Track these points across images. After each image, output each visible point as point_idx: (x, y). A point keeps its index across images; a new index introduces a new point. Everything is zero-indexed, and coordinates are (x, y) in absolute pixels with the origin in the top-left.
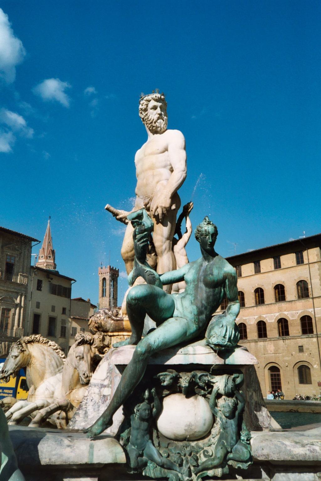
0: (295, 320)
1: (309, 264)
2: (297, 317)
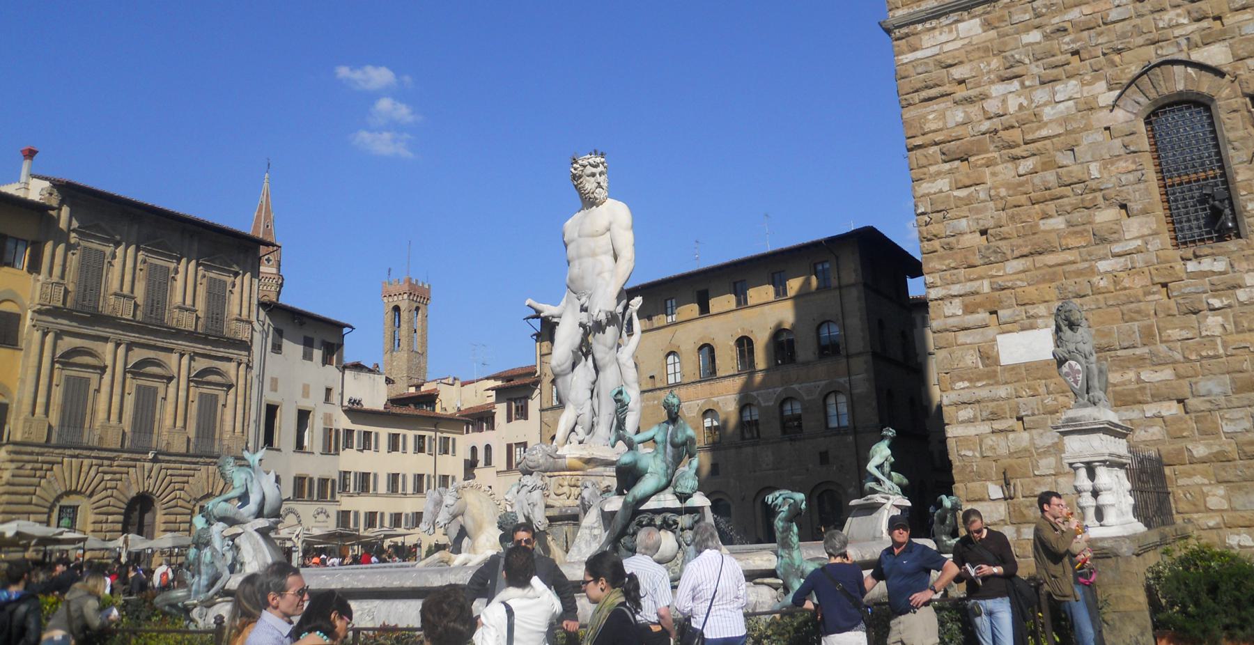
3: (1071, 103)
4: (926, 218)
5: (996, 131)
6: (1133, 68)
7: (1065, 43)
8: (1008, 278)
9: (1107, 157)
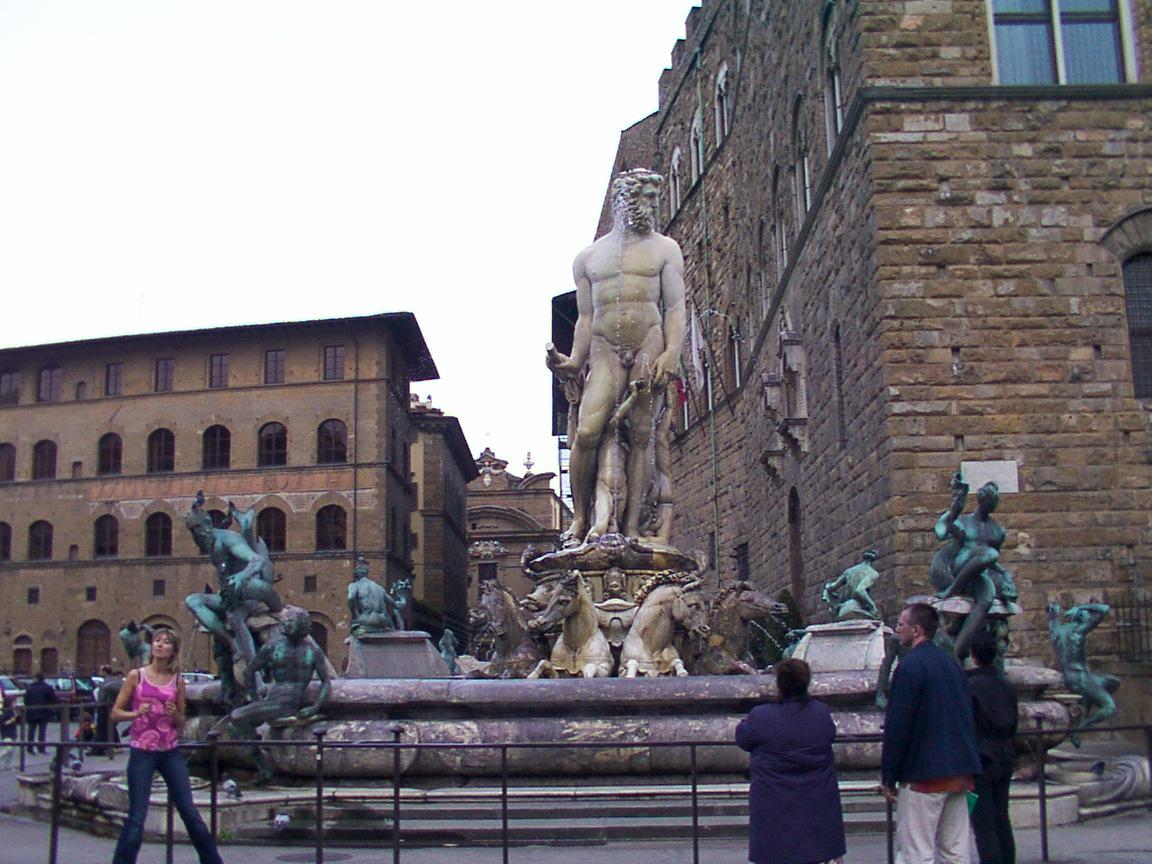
0: (305, 513)
1: (357, 381)
2: (310, 507)
3: (1057, 230)
4: (896, 323)
5: (980, 242)
6: (1120, 208)
7: (1057, 166)
8: (978, 402)
9: (1086, 293)
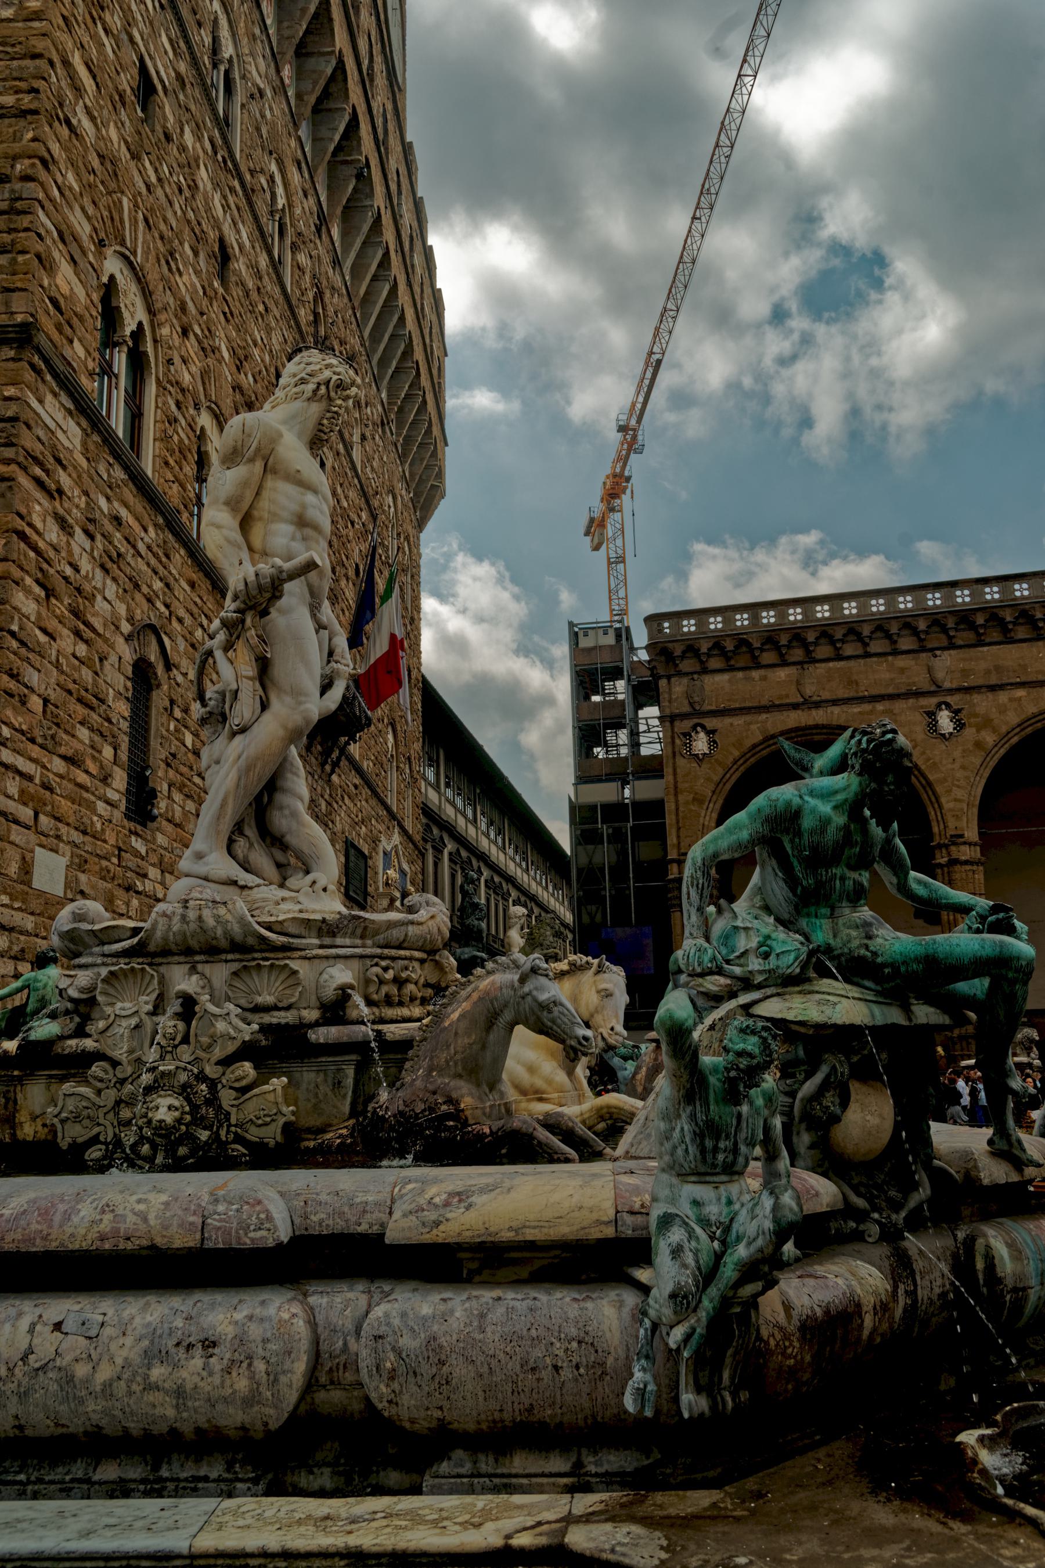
4: (15, 644)
